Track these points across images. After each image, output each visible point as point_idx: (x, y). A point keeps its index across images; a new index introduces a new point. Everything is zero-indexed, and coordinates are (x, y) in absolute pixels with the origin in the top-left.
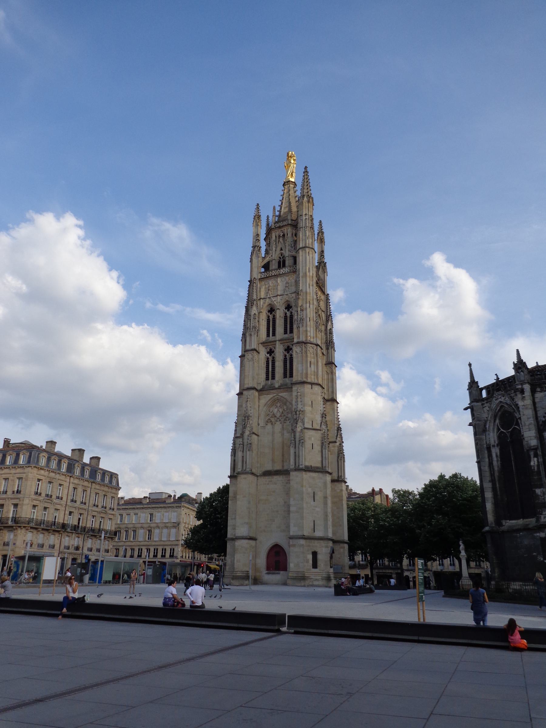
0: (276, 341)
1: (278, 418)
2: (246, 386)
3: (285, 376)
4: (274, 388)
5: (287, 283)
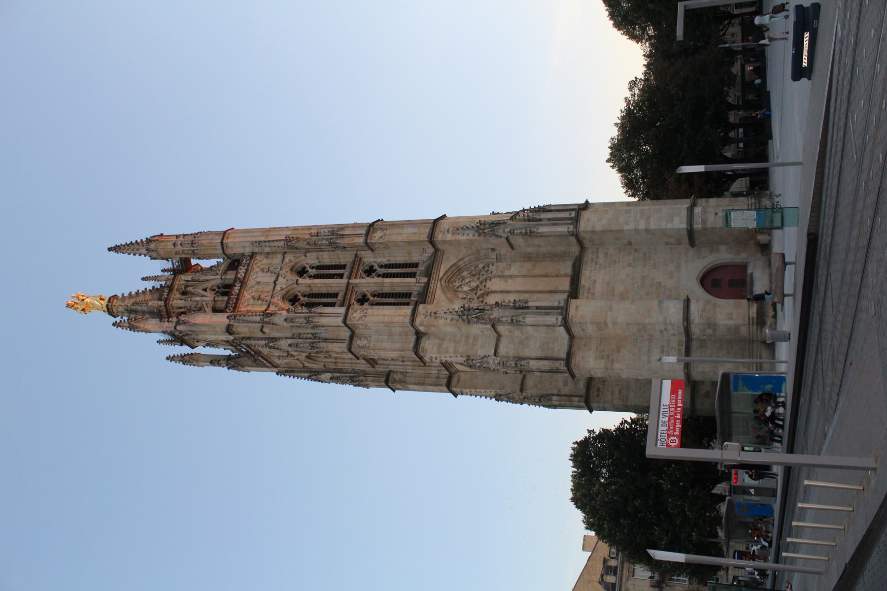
0: (348, 284)
1: (481, 283)
2: (408, 320)
3: (413, 275)
4: (428, 284)
5: (263, 271)
